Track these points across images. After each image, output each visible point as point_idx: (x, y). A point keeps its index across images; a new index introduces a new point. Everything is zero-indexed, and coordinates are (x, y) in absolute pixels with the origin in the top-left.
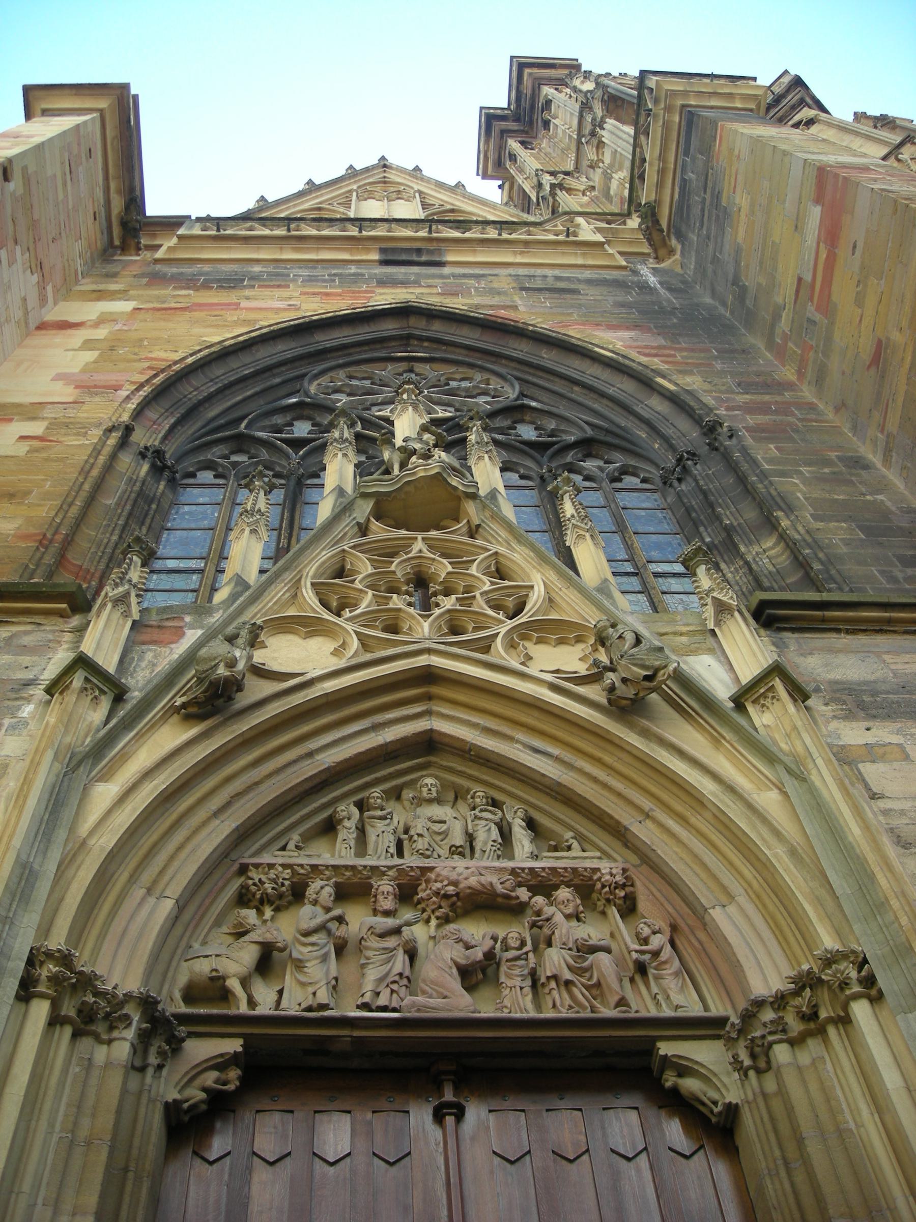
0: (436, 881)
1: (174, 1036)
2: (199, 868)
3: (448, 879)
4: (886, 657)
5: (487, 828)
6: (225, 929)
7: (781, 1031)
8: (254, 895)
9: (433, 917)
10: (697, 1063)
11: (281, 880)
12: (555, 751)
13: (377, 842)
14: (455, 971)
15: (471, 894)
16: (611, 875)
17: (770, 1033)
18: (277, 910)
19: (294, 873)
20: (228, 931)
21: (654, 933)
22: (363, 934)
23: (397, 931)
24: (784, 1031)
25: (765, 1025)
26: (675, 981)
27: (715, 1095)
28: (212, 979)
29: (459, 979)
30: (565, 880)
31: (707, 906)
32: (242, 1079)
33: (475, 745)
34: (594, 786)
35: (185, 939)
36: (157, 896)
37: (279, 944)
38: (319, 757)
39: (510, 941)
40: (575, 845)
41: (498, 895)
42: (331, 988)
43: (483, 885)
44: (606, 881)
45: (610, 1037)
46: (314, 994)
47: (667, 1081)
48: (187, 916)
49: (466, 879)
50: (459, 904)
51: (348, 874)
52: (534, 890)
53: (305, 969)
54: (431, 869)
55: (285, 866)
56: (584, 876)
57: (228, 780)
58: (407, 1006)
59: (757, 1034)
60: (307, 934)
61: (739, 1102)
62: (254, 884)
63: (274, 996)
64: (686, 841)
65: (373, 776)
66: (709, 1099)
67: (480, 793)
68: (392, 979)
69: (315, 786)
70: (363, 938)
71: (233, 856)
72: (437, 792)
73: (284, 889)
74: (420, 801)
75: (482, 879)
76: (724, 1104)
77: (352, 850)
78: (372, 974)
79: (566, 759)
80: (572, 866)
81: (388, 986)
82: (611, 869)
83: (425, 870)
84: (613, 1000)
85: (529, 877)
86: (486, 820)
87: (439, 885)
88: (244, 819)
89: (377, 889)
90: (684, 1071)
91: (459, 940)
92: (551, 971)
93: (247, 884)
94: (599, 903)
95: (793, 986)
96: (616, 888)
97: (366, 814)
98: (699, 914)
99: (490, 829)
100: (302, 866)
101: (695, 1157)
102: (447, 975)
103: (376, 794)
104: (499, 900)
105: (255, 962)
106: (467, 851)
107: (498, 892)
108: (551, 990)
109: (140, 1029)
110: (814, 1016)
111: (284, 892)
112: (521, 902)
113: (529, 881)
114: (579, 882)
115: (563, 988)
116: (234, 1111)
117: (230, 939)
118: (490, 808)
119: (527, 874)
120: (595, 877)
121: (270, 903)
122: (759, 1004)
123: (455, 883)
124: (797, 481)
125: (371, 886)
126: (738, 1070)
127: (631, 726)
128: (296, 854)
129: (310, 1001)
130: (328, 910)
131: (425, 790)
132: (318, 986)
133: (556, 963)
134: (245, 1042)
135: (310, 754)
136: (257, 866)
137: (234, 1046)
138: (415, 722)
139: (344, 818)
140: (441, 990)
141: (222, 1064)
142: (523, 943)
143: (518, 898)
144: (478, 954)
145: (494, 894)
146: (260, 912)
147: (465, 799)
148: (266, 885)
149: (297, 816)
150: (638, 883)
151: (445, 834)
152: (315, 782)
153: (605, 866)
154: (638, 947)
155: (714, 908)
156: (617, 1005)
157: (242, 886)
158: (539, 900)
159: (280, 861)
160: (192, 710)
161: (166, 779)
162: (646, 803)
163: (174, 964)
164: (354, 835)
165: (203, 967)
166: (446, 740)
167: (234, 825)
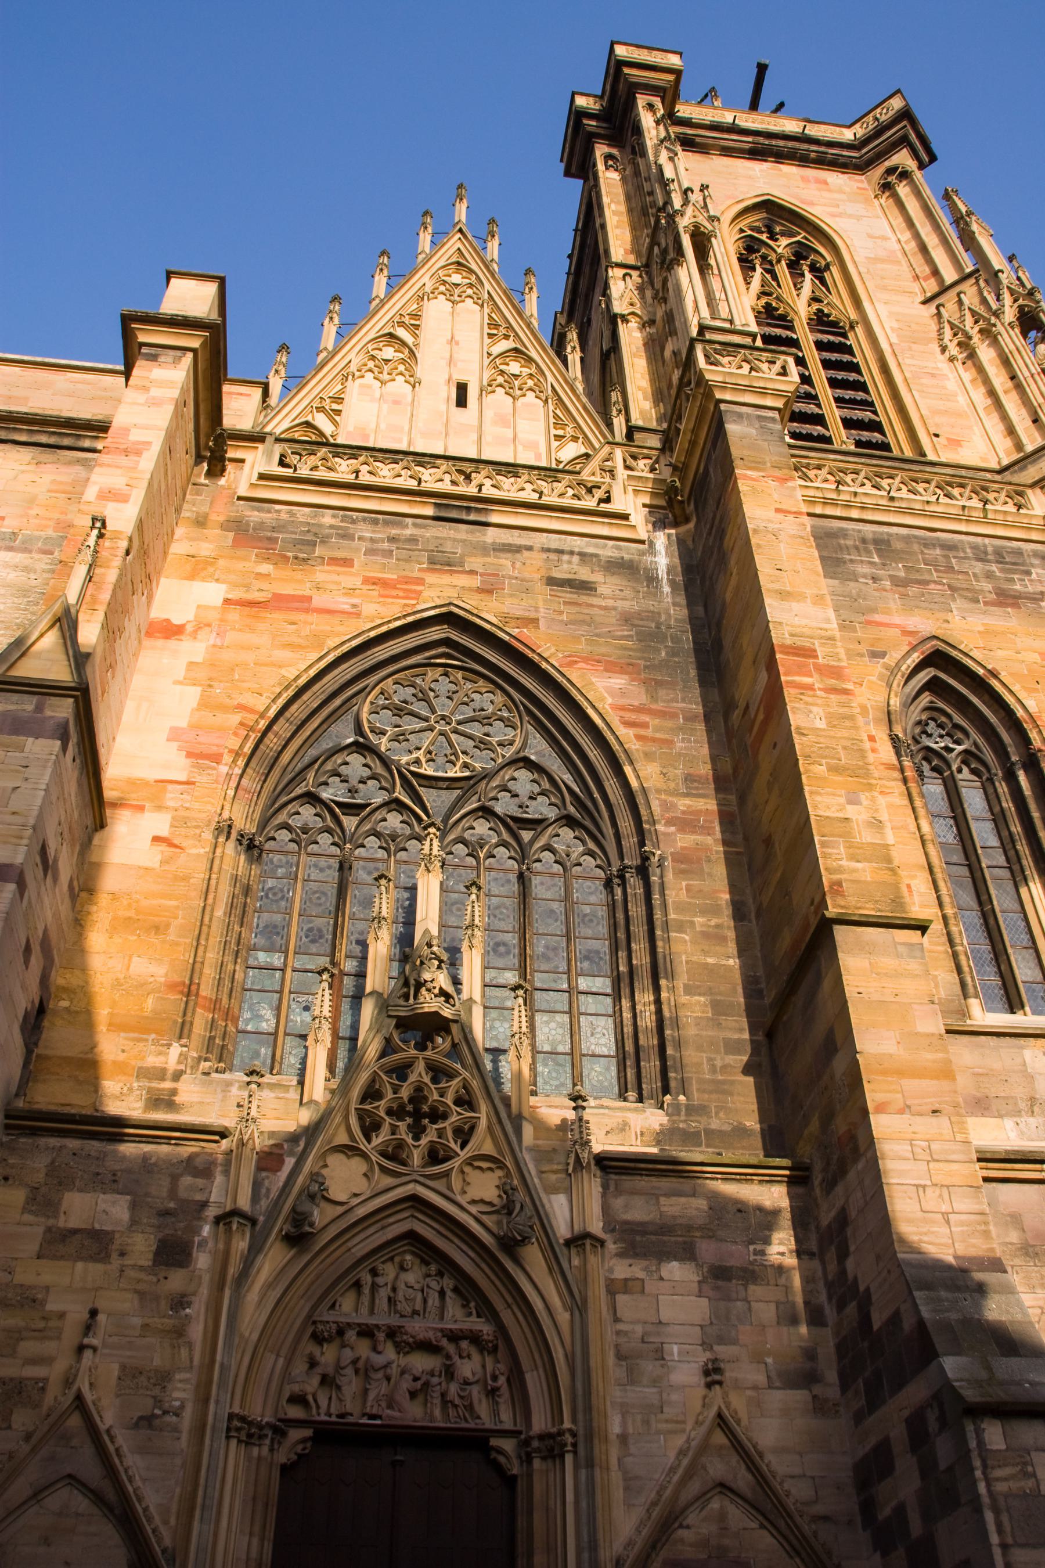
4: (662, 1200)
16: (488, 1335)
40: (474, 1312)
55: (334, 1322)
83: (400, 1327)
87: (405, 1337)
90: (500, 1451)
98: (520, 1374)
123: (412, 1337)
124: (687, 938)
129: (343, 1411)
135: (349, 1250)
136: (321, 1322)
137: (308, 1433)
141: (304, 1440)
144: (418, 1385)
151: (414, 1300)
158: (451, 1348)
159: (331, 1319)
165: (296, 1388)
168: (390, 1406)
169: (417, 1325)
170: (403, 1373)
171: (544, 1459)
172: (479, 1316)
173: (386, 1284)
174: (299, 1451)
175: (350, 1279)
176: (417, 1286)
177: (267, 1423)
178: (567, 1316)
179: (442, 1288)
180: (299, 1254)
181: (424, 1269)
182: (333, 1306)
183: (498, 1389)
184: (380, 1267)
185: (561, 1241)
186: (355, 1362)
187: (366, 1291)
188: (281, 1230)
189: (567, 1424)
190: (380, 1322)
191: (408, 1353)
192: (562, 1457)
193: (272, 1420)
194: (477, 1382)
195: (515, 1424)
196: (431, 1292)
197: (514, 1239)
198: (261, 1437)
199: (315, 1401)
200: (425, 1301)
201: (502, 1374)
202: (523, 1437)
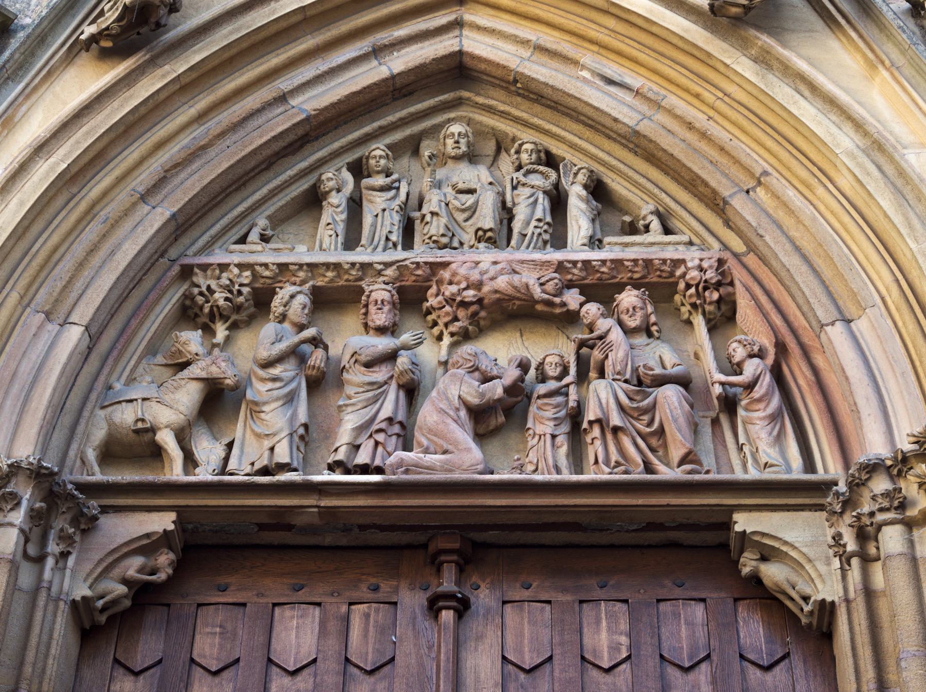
0: (451, 283)
1: (82, 514)
2: (118, 279)
3: (467, 279)
5: (532, 199)
6: (160, 359)
7: (896, 508)
8: (201, 308)
9: (445, 333)
10: (786, 543)
11: (237, 287)
13: (374, 226)
14: (463, 413)
15: (499, 300)
16: (701, 269)
17: (881, 510)
18: (234, 327)
19: (255, 276)
20: (165, 362)
21: (751, 356)
23: (391, 357)
25: (874, 498)
26: (769, 427)
27: (808, 590)
28: (137, 432)
29: (469, 425)
33: (522, 74)
35: (102, 378)
36: (61, 321)
37: (228, 381)
38: (294, 102)
39: (547, 367)
40: (655, 225)
41: (537, 302)
42: (296, 439)
43: (515, 288)
44: (692, 278)
45: (668, 505)
46: (272, 449)
48: (105, 343)
49: (492, 279)
50: (483, 314)
51: (330, 274)
52: (590, 293)
54: (445, 265)
55: (241, 266)
56: (662, 271)
57: (160, 145)
58: (391, 465)
59: (866, 509)
60: (267, 364)
61: (836, 600)
62: (201, 294)
63: (220, 451)
65: (376, 125)
68: (377, 427)
69: (290, 145)
70: (344, 367)
71: (173, 253)
72: (469, 145)
73: (241, 299)
74: (441, 159)
75: (516, 279)
76: (815, 601)
77: (340, 239)
78: (350, 421)
80: (645, 256)
81: (371, 436)
83: (435, 267)
85: (583, 274)
87: (454, 289)
88: (183, 203)
89: (369, 296)
91: (475, 369)
93: (191, 294)
94: (683, 309)
95: (916, 447)
97: (366, 182)
99: (536, 201)
100: (266, 265)
101: (777, 670)
102: (449, 421)
103: (378, 153)
104: (539, 307)
105: (197, 406)
108: (593, 439)
109: (32, 510)
111: (242, 304)
112: (568, 310)
113: (584, 279)
114: (655, 279)
115: (609, 437)
116: (168, 605)
117: (167, 372)
118: (541, 168)
119: (581, 270)
120: (678, 273)
121: (224, 318)
122: (872, 468)
126: (841, 556)
127: (744, 45)
128: (259, 248)
130: (301, 328)
131: (450, 142)
132: (277, 438)
133: (604, 401)
134: (178, 516)
135: (282, 99)
136: (205, 267)
137: (164, 522)
138: (438, 39)
139: (331, 191)
140: (440, 442)
142: (565, 372)
143: (564, 304)
144: (496, 389)
145: (531, 301)
146: (208, 331)
147: (507, 151)
148: (217, 295)
149: (264, 191)
151: (473, 210)
152: (291, 137)
153: (693, 256)
154: (723, 378)
155: (833, 324)
156: (681, 463)
158: (592, 309)
159: (236, 259)
160: (107, 44)
161: (66, 156)
163: (86, 414)
164: (344, 216)
165: (126, 416)
166: (483, 66)
167: (168, 214)
172: (667, 231)
179: (557, 186)
195: (809, 465)
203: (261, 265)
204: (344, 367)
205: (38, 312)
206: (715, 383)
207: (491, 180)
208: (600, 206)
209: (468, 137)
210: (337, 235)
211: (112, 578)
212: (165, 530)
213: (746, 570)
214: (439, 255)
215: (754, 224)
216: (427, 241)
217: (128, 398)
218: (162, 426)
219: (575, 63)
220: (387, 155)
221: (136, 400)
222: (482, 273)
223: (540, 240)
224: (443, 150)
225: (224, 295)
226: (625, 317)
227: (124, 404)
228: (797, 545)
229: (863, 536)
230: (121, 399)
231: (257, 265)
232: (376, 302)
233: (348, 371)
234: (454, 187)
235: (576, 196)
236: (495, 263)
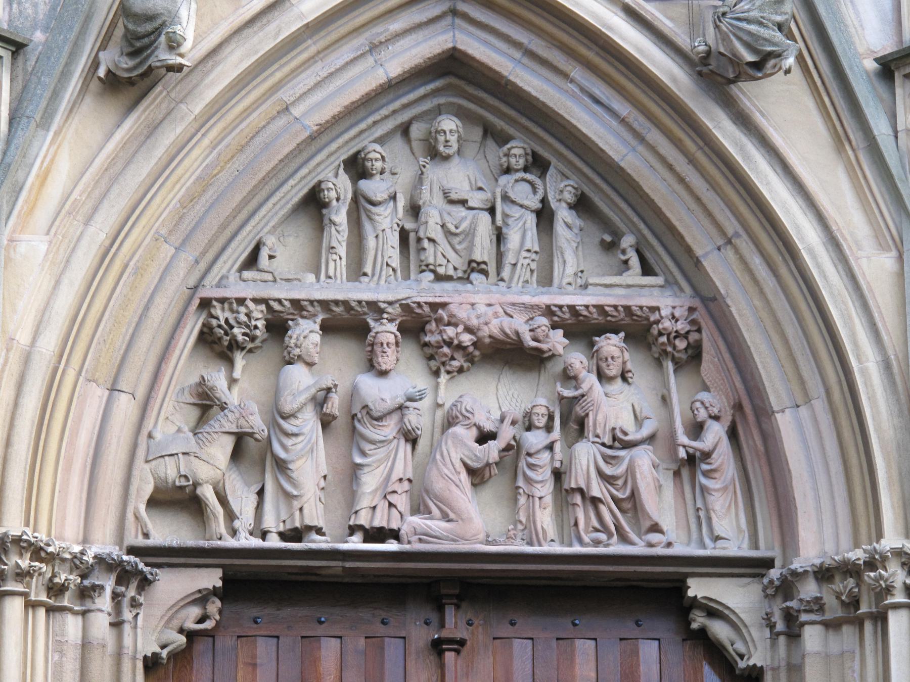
0: (449, 324)
8: (220, 339)
9: (442, 370)
10: (728, 608)
12: (623, 108)
14: (464, 475)
17: (806, 611)
19: (269, 308)
22: (356, 409)
24: (821, 609)
25: (801, 600)
30: (613, 320)
31: (775, 408)
32: (220, 612)
34: (667, 175)
37: (257, 436)
39: (535, 418)
40: (635, 261)
44: (664, 329)
46: (301, 509)
47: (694, 621)
53: (289, 472)
54: (444, 305)
55: (256, 301)
63: (253, 499)
64: (770, 297)
66: (734, 650)
67: (517, 150)
74: (434, 154)
79: (636, 125)
82: (674, 308)
83: (434, 306)
84: (647, 524)
85: (567, 316)
86: (521, 206)
87: (450, 332)
89: (374, 337)
90: (713, 612)
92: (576, 481)
94: (654, 349)
96: (675, 337)
99: (525, 223)
100: (279, 301)
102: (454, 488)
106: (492, 268)
107: (526, 345)
110: (855, 603)
115: (588, 503)
118: (528, 176)
119: (563, 313)
125: (368, 329)
131: (441, 138)
134: (224, 574)
136: (222, 301)
137: (212, 579)
144: (493, 449)
148: (236, 331)
150: (705, 335)
155: (783, 411)
157: (204, 325)
158: (577, 359)
162: (731, 226)
163: (136, 473)
165: (170, 471)
167: (191, 259)
168: (418, 508)
169: (481, 299)
170: (450, 422)
171: (832, 625)
173: (393, 198)
174: (191, 625)
175: (296, 190)
176: (476, 199)
177: (100, 559)
178: (887, 261)
179: (544, 201)
180: (153, 129)
181: (494, 153)
182: (252, 261)
183: (707, 455)
184: (375, 151)
185: (871, 65)
186: (320, 400)
187: (340, 216)
188: (96, 64)
189: (891, 540)
190: (381, 295)
191: (461, 370)
192: (880, 619)
193: (114, 551)
194: (651, 439)
196: (515, 212)
197: (734, 61)
198: (85, 593)
199: (223, 500)
200: (499, 237)
201: (716, 418)
202: (774, 574)
203: (275, 300)
204: (356, 415)
205: (90, 381)
206: (679, 445)
207: (480, 184)
208: (582, 224)
209: (458, 132)
210: (340, 258)
211: (171, 628)
212: (214, 587)
213: (694, 626)
214: (438, 295)
215: (722, 291)
216: (424, 268)
217: (169, 453)
218: (201, 481)
219: (565, 75)
220: (383, 157)
221: (177, 454)
222: (478, 317)
223: (528, 270)
224: (433, 144)
225: (243, 331)
226: (603, 365)
227: (167, 458)
228: (737, 611)
229: (790, 617)
230: (163, 454)
231: (271, 299)
232: (382, 344)
233: (359, 421)
234: (446, 194)
235: (563, 215)
236: (490, 305)
